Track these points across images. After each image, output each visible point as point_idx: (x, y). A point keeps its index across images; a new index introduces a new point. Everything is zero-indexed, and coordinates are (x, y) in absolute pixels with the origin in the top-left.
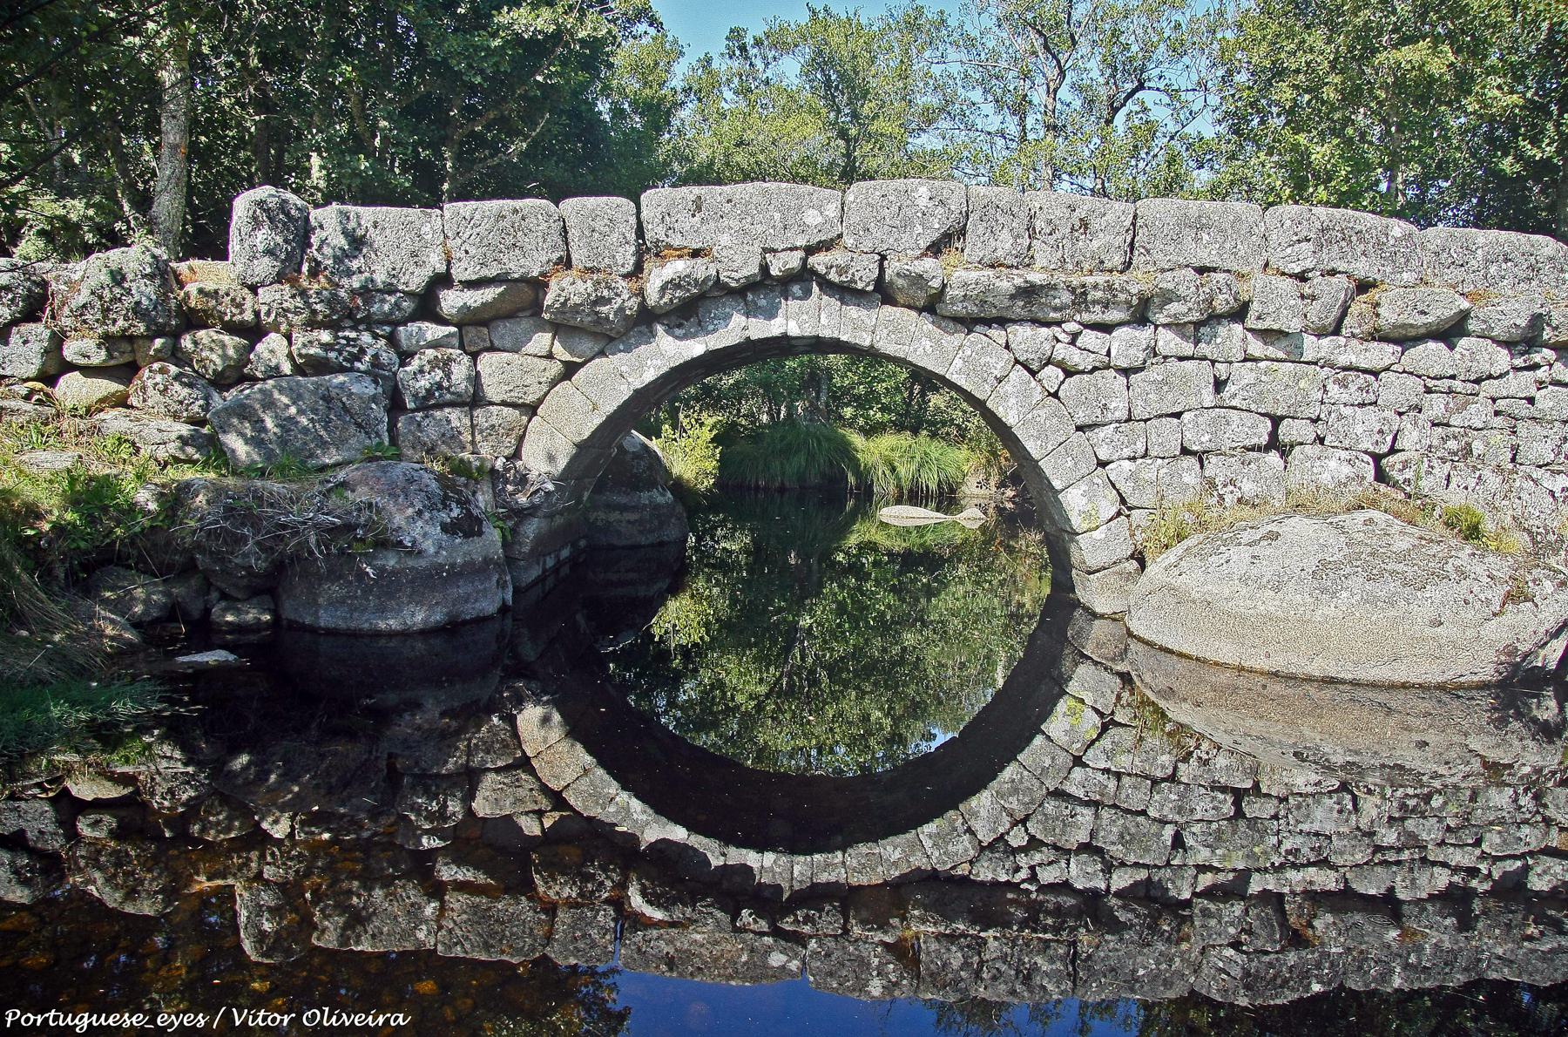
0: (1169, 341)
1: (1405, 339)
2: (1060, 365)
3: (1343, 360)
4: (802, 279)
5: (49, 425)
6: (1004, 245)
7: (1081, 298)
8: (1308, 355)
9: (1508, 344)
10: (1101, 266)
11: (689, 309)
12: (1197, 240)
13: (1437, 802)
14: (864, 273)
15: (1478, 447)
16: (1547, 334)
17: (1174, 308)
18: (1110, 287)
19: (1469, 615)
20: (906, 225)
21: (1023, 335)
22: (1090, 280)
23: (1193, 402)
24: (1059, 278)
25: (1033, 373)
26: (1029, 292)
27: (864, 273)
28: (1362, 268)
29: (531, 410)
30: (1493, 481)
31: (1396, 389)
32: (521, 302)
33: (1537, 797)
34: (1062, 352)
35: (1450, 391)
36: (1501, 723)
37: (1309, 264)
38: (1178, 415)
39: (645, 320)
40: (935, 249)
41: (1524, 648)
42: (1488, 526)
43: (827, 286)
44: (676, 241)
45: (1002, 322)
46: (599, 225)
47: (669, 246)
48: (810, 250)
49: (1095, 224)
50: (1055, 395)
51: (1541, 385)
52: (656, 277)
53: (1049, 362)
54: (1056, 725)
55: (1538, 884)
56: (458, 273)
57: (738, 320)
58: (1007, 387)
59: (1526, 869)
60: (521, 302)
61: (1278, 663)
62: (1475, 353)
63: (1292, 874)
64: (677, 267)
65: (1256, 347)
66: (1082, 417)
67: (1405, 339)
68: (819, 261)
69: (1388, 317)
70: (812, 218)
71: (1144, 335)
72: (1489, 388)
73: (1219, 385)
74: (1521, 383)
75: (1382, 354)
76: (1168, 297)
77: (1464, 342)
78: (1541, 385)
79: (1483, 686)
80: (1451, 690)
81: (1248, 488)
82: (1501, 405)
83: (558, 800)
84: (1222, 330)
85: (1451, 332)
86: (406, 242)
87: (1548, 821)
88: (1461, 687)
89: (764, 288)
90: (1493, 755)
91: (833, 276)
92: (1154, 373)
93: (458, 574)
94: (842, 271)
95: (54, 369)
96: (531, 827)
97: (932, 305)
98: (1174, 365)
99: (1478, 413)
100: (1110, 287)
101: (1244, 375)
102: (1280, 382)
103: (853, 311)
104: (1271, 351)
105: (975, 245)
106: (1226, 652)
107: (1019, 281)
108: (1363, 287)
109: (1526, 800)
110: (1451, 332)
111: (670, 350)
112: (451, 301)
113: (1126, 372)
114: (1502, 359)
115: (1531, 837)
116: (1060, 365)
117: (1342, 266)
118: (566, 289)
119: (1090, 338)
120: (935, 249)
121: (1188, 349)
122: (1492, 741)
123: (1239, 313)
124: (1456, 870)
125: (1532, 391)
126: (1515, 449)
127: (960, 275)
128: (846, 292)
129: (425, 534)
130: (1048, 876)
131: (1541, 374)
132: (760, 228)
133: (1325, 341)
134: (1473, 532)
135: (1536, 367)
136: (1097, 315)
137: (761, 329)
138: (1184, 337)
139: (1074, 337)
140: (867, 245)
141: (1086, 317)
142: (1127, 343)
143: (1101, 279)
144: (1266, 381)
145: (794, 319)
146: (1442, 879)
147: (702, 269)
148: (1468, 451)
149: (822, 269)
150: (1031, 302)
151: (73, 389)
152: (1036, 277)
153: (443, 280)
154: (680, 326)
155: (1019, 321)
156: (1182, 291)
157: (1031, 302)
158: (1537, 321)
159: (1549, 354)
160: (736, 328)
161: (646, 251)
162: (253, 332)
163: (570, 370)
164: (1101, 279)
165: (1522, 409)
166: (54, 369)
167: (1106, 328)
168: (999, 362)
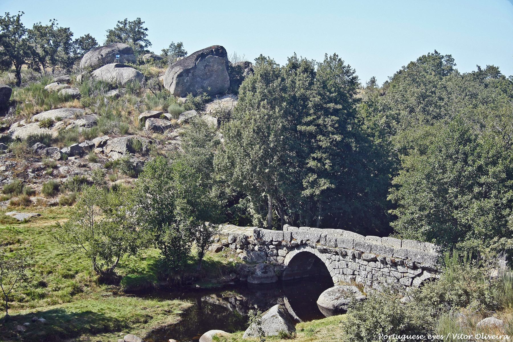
1: (369, 261)
8: (357, 262)
21: (327, 254)
28: (362, 250)
29: (285, 257)
31: (368, 269)
48: (307, 240)
52: (292, 242)
56: (274, 240)
62: (379, 264)
73: (347, 265)
74: (386, 270)
75: (365, 263)
85: (375, 260)
93: (262, 278)
95: (236, 249)
102: (354, 265)
108: (363, 253)
110: (375, 260)
111: (296, 252)
112: (274, 243)
114: (382, 266)
118: (284, 243)
137: (305, 250)
145: (308, 249)
153: (272, 241)
160: (302, 250)
163: (288, 253)
166: (236, 249)
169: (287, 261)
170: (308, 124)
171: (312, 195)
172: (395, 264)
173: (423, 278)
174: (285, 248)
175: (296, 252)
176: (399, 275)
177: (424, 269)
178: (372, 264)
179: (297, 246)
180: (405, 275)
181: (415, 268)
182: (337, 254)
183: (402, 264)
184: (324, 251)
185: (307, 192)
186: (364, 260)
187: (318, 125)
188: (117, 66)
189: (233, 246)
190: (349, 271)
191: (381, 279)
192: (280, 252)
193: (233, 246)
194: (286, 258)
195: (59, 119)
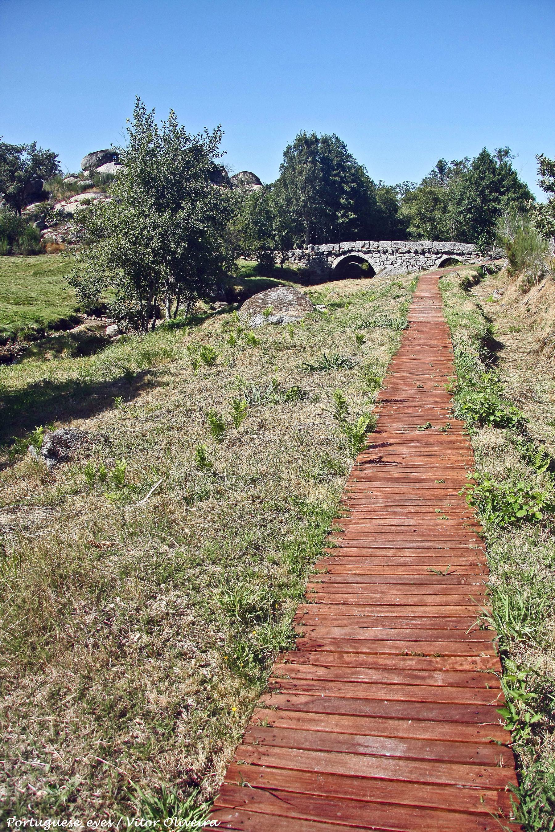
1: (404, 253)
4: (352, 250)
5: (294, 265)
14: (357, 249)
31: (404, 258)
32: (330, 254)
39: (339, 255)
60: (330, 254)
74: (417, 257)
85: (409, 252)
86: (324, 248)
89: (349, 251)
95: (295, 260)
99: (412, 260)
110: (409, 252)
123: (387, 251)
127: (364, 250)
129: (319, 272)
145: (353, 254)
151: (297, 261)
161: (340, 248)
162: (310, 256)
166: (295, 260)
169: (334, 266)
170: (335, 176)
171: (343, 222)
172: (423, 253)
173: (442, 259)
176: (425, 259)
177: (443, 253)
178: (407, 255)
179: (344, 253)
181: (437, 253)
182: (379, 252)
183: (429, 252)
184: (366, 253)
185: (340, 221)
187: (341, 177)
188: (115, 164)
189: (293, 259)
190: (389, 262)
191: (415, 263)
192: (330, 259)
193: (293, 259)
194: (335, 262)
195: (95, 199)
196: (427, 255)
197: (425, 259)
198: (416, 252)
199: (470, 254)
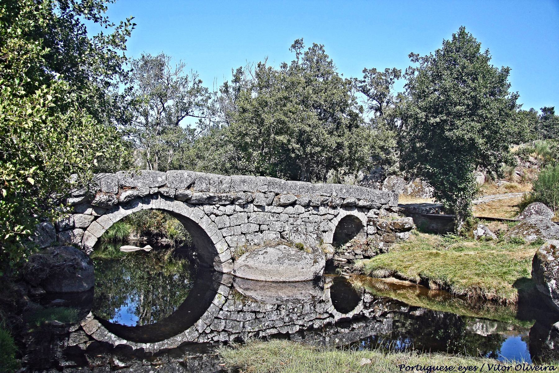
0: (238, 208)
1: (285, 206)
2: (215, 214)
3: (273, 211)
6: (204, 186)
7: (220, 199)
9: (304, 206)
10: (224, 192)
11: (129, 204)
12: (244, 185)
13: (296, 310)
15: (300, 229)
16: (311, 204)
17: (240, 201)
18: (227, 196)
19: (308, 266)
20: (182, 182)
21: (207, 208)
22: (222, 195)
23: (243, 222)
24: (216, 195)
25: (208, 216)
26: (210, 198)
27: (172, 193)
28: (277, 191)
30: (303, 237)
33: (314, 307)
34: (215, 211)
35: (294, 217)
36: (315, 287)
37: (266, 190)
38: (240, 225)
40: (189, 187)
41: (318, 272)
42: (305, 247)
43: (163, 196)
44: (128, 185)
45: (202, 205)
46: (109, 181)
47: (125, 186)
48: (159, 187)
49: (224, 182)
50: (214, 222)
51: (310, 214)
53: (212, 213)
54: (216, 301)
55: (316, 326)
57: (140, 204)
58: (203, 220)
59: (313, 324)
61: (274, 279)
63: (268, 331)
64: (129, 192)
65: (256, 209)
66: (220, 227)
67: (285, 206)
68: (162, 190)
69: (282, 201)
70: (160, 179)
71: (233, 207)
72: (301, 216)
73: (248, 218)
74: (306, 215)
75: (280, 209)
76: (239, 198)
77: (296, 206)
78: (310, 214)
79: (311, 280)
80: (306, 282)
81: (256, 241)
82: (303, 219)
83: (90, 337)
84: (249, 205)
85: (293, 204)
87: (316, 312)
88: (308, 281)
90: (314, 294)
91: (165, 194)
92: (235, 216)
94: (167, 193)
96: (83, 346)
97: (187, 200)
98: (239, 214)
99: (299, 222)
100: (227, 196)
101: (253, 215)
103: (168, 202)
104: (259, 210)
105: (197, 187)
106: (262, 278)
107: (208, 196)
108: (277, 194)
109: (312, 308)
110: (293, 204)
113: (229, 216)
114: (303, 210)
115: (313, 316)
116: (215, 214)
117: (273, 190)
118: (101, 198)
119: (221, 208)
120: (189, 187)
121: (242, 210)
122: (313, 291)
124: (300, 325)
125: (309, 216)
126: (306, 229)
127: (194, 194)
128: (167, 198)
130: (215, 339)
131: (310, 212)
132: (148, 182)
133: (269, 207)
134: (302, 249)
135: (309, 211)
136: (223, 203)
137: (146, 207)
138: (241, 207)
139: (218, 207)
140: (173, 186)
141: (221, 203)
142: (229, 209)
143: (225, 195)
144: (257, 216)
146: (298, 328)
147: (135, 193)
148: (298, 230)
149: (162, 192)
150: (210, 201)
152: (212, 195)
154: (126, 206)
155: (206, 204)
156: (242, 197)
157: (210, 201)
158: (310, 201)
159: (312, 208)
163: (96, 218)
164: (225, 195)
165: (307, 220)
167: (225, 205)
168: (201, 214)
174: (89, 211)
175: (122, 212)
178: (290, 209)
180: (326, 216)
186: (280, 205)
192: (78, 219)
196: (322, 210)
197: (319, 218)
198: (307, 206)
199: (379, 208)
